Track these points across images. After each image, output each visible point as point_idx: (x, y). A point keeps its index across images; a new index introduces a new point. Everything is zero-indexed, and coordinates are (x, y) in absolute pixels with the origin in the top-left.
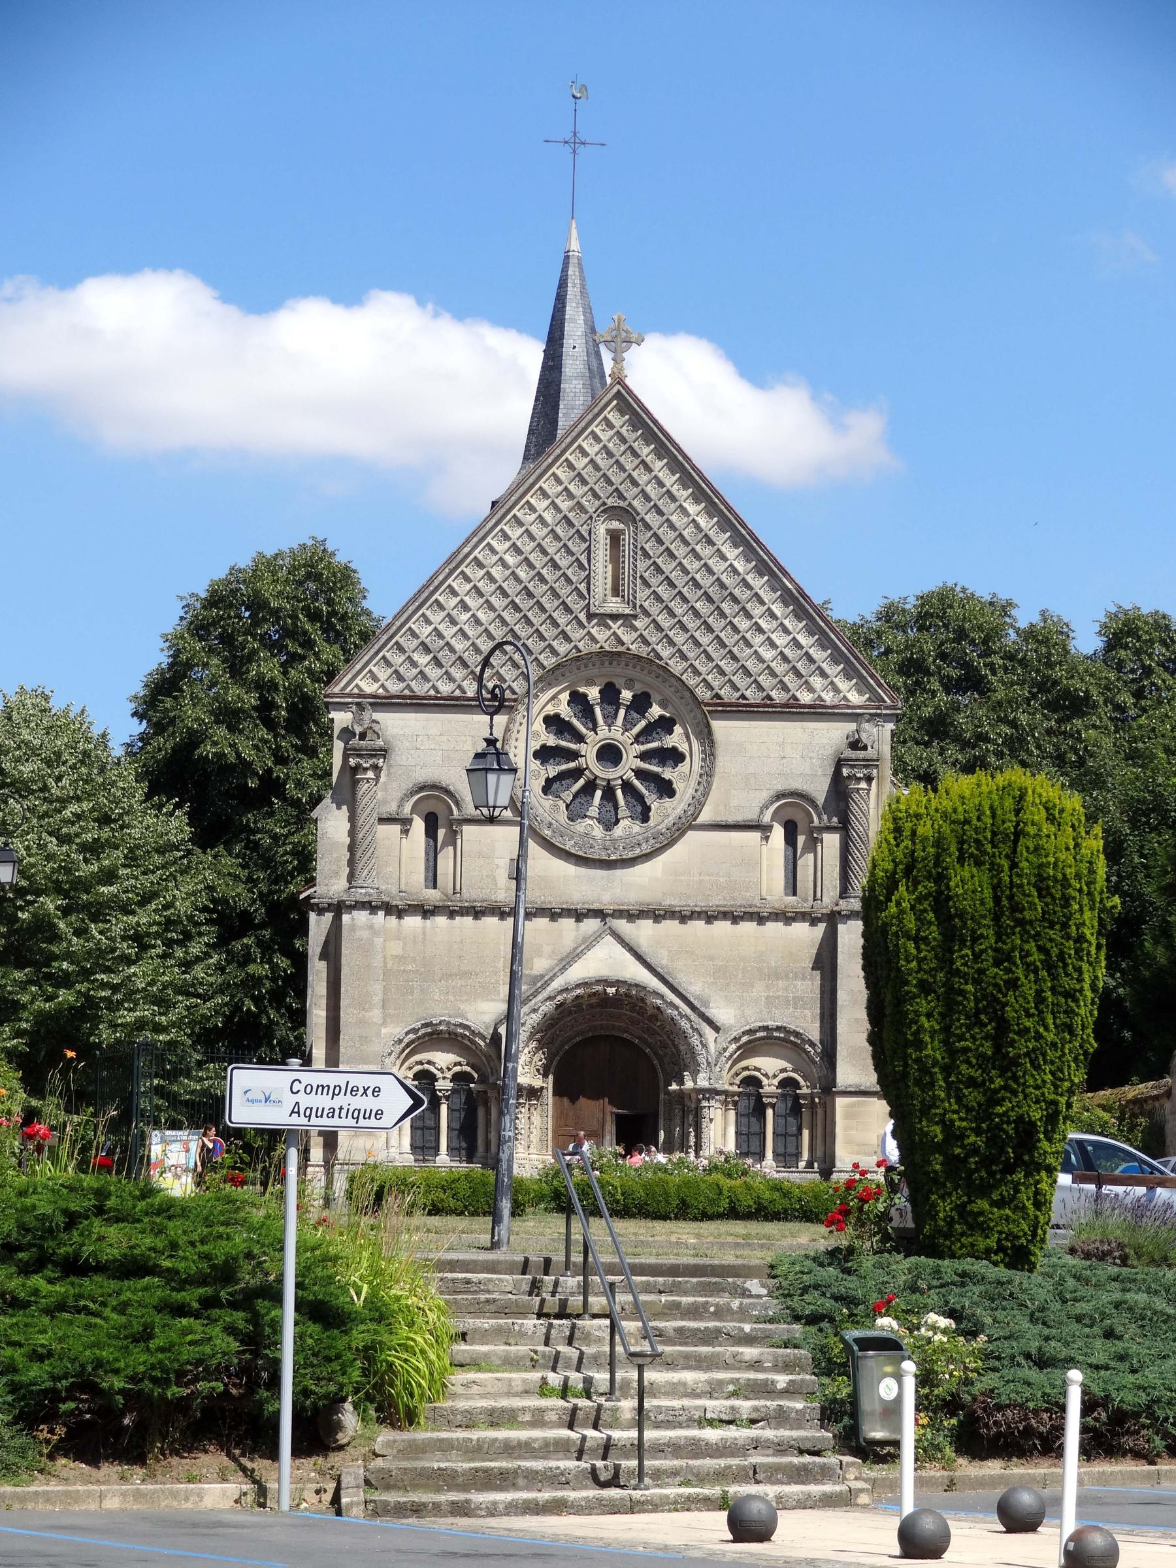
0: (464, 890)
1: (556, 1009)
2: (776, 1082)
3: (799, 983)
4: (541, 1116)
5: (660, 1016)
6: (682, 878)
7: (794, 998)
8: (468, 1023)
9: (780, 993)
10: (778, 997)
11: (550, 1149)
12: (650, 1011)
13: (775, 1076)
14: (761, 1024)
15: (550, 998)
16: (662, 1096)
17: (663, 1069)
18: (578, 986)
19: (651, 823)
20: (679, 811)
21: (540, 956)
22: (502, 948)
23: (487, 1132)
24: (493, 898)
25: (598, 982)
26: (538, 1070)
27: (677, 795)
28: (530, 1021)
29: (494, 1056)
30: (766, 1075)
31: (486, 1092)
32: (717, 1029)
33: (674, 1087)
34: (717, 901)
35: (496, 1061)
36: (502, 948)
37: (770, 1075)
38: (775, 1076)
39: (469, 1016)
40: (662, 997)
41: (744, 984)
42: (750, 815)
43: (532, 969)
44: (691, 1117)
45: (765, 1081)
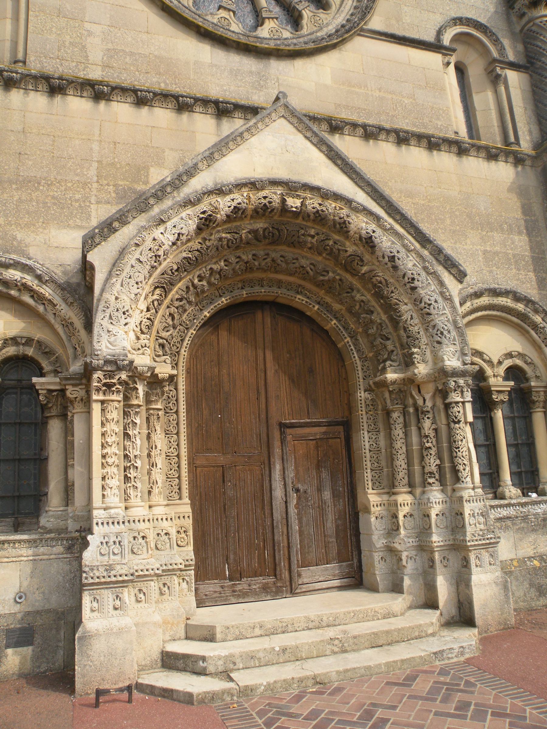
0: (31, 58)
1: (199, 229)
2: (501, 370)
3: (516, 238)
4: (167, 433)
5: (367, 257)
6: (357, 90)
7: (514, 256)
8: (29, 262)
9: (497, 248)
10: (496, 253)
11: (185, 492)
12: (351, 249)
13: (500, 363)
14: (485, 286)
15: (189, 203)
16: (362, 395)
17: (358, 351)
18: (239, 186)
19: (305, 31)
20: (341, 19)
21: (160, 164)
22: (95, 146)
23: (67, 466)
24: (81, 75)
25: (274, 183)
26: (162, 346)
27: (334, 8)
28: (149, 243)
29: (78, 323)
30: (490, 362)
31: (63, 391)
32: (460, 276)
33: (391, 376)
34: (404, 124)
35: (83, 333)
36: (95, 146)
37: (495, 361)
38: (500, 363)
39: (32, 251)
40: (377, 218)
41: (454, 232)
42: (429, 37)
43: (146, 183)
44: (427, 424)
45: (489, 371)
